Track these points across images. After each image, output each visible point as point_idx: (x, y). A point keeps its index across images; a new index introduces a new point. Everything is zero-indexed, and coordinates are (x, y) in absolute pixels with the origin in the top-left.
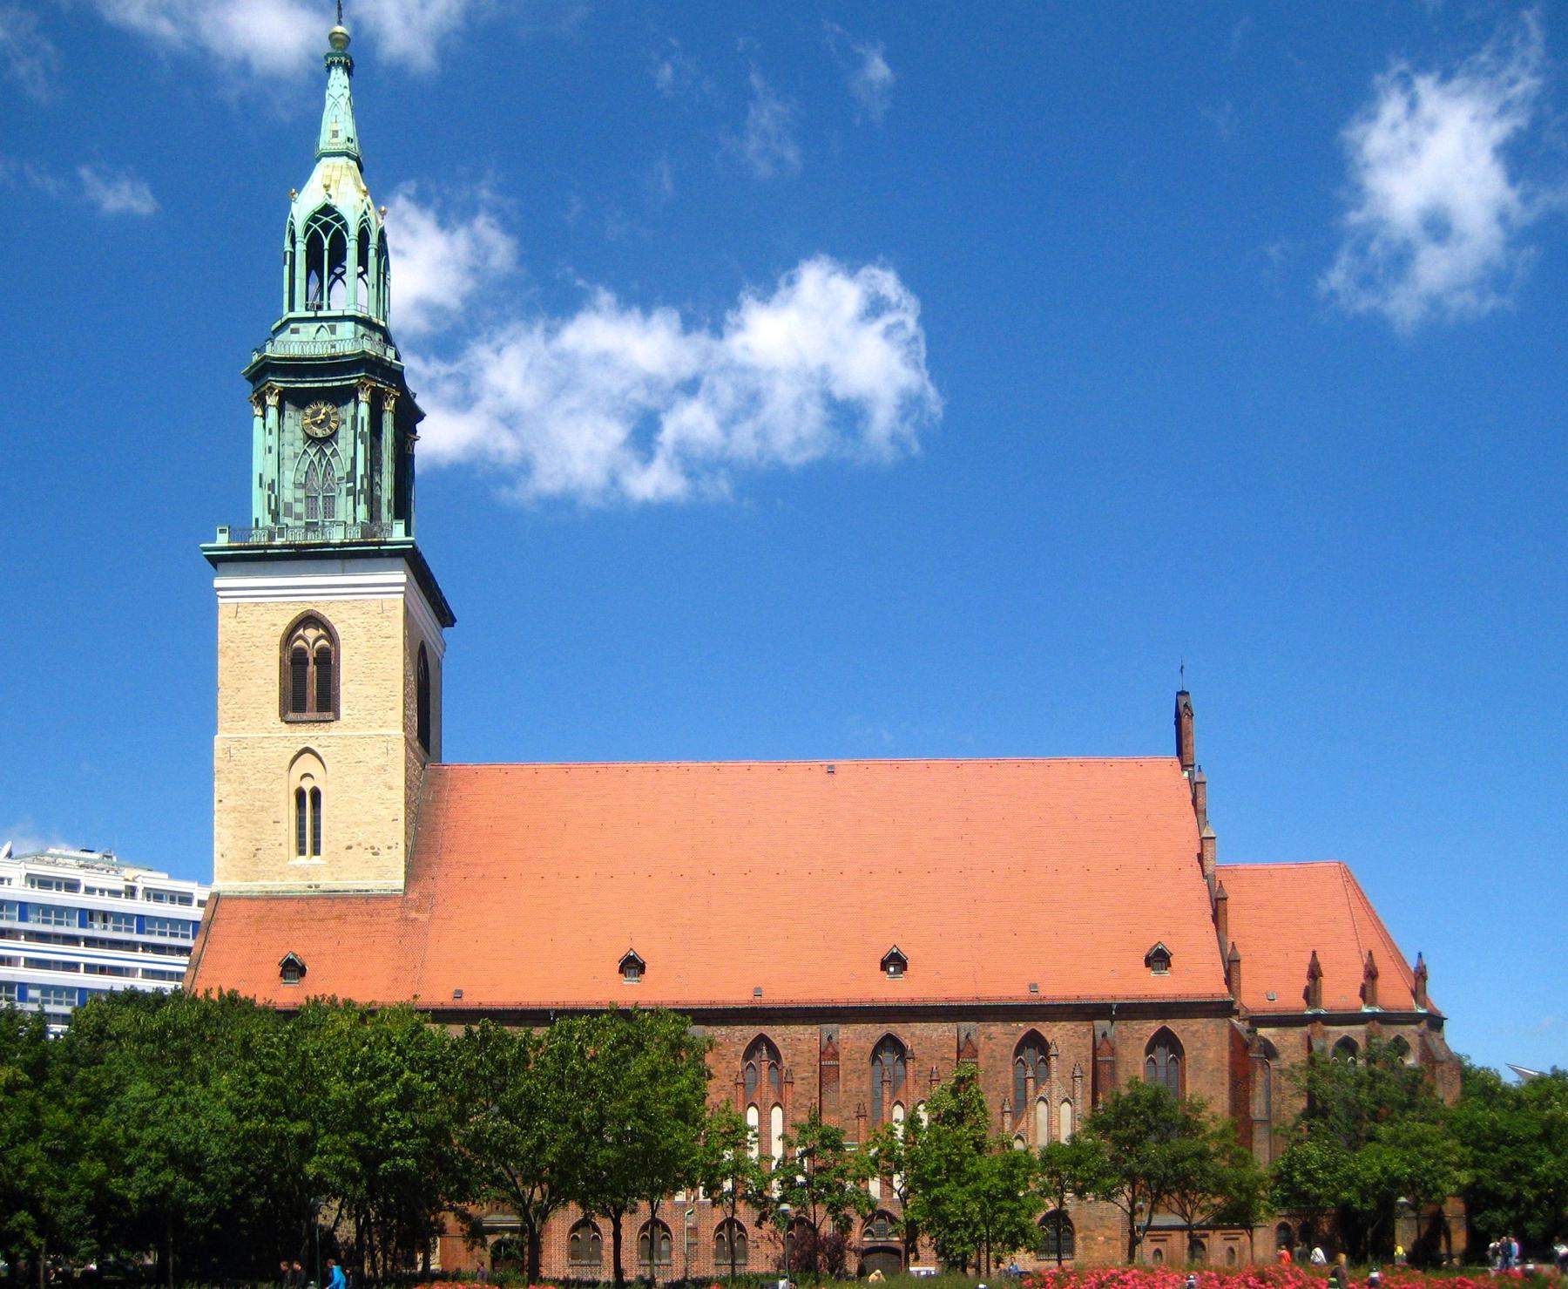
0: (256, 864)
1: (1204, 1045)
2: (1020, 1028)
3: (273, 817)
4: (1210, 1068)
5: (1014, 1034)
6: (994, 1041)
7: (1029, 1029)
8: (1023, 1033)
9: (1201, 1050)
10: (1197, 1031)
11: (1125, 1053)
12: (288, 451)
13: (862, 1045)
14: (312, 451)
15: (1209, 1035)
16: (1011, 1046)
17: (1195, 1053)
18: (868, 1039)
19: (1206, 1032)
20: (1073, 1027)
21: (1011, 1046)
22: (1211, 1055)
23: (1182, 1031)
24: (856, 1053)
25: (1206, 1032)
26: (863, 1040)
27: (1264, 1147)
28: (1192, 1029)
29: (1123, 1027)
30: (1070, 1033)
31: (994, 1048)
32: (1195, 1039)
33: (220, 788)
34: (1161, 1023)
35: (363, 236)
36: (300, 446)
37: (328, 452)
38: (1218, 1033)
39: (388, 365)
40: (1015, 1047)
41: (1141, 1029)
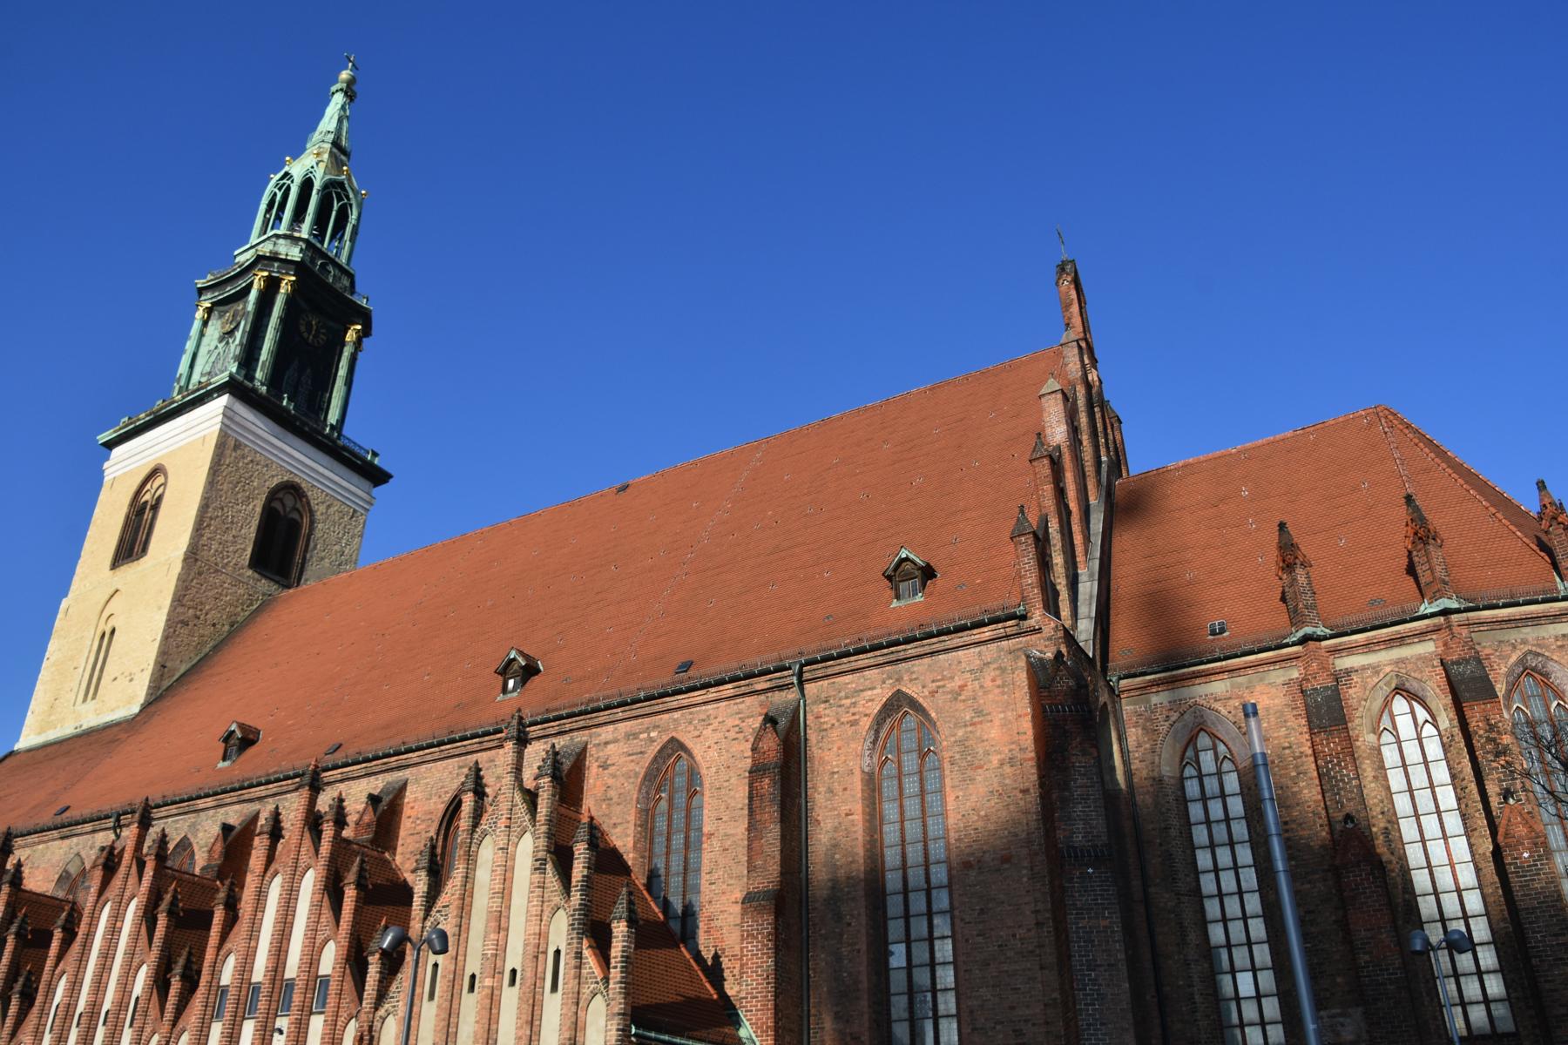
0: (50, 715)
1: (979, 712)
2: (652, 740)
3: (75, 665)
4: (995, 759)
5: (641, 753)
6: (612, 769)
7: (665, 738)
8: (656, 747)
9: (973, 724)
10: (962, 687)
11: (828, 756)
12: (203, 351)
13: (432, 806)
14: (220, 346)
15: (986, 693)
16: (636, 775)
17: (960, 733)
18: (440, 797)
19: (982, 687)
20: (737, 722)
21: (636, 775)
22: (993, 732)
23: (933, 693)
24: (424, 821)
25: (982, 687)
26: (435, 799)
27: (1104, 923)
28: (950, 686)
29: (823, 706)
30: (732, 734)
31: (610, 782)
32: (961, 706)
33: (53, 646)
34: (893, 686)
35: (307, 184)
36: (215, 342)
37: (231, 341)
38: (1003, 686)
39: (283, 257)
40: (641, 776)
41: (854, 704)
